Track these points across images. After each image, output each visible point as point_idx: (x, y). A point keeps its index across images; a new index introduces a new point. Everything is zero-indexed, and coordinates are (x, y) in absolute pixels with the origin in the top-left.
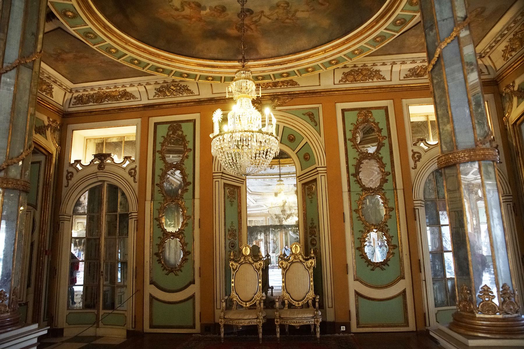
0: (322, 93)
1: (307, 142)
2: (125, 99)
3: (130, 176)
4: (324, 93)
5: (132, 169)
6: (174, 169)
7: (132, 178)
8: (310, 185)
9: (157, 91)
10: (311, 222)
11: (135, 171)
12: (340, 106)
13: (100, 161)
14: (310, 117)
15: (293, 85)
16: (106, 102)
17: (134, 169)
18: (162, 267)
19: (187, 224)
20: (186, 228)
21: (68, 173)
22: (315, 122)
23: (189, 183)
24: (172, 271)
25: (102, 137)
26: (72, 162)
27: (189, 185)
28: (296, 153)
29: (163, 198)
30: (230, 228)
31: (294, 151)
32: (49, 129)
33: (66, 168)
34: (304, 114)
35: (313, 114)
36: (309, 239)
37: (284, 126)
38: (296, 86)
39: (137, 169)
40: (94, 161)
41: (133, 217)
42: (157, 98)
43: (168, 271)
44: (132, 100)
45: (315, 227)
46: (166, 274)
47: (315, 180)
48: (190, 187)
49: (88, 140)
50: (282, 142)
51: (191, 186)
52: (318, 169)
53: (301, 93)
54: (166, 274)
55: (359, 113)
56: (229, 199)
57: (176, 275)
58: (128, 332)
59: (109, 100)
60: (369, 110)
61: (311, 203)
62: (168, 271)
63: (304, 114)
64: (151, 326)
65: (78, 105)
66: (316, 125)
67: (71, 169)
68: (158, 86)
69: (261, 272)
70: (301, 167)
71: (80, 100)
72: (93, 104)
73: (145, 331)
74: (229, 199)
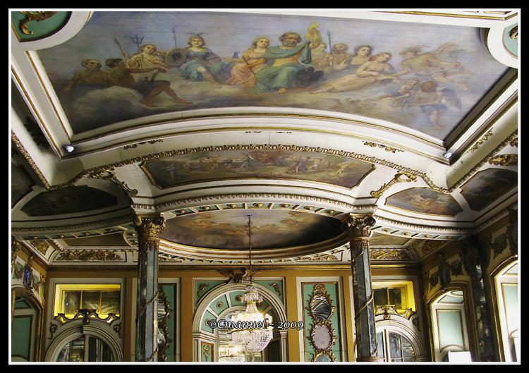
5: (117, 325)
11: (120, 328)
12: (300, 280)
21: (52, 325)
22: (279, 292)
26: (56, 315)
33: (49, 320)
39: (122, 326)
55: (314, 287)
60: (322, 284)
66: (280, 295)
67: (54, 322)
71: (66, 256)
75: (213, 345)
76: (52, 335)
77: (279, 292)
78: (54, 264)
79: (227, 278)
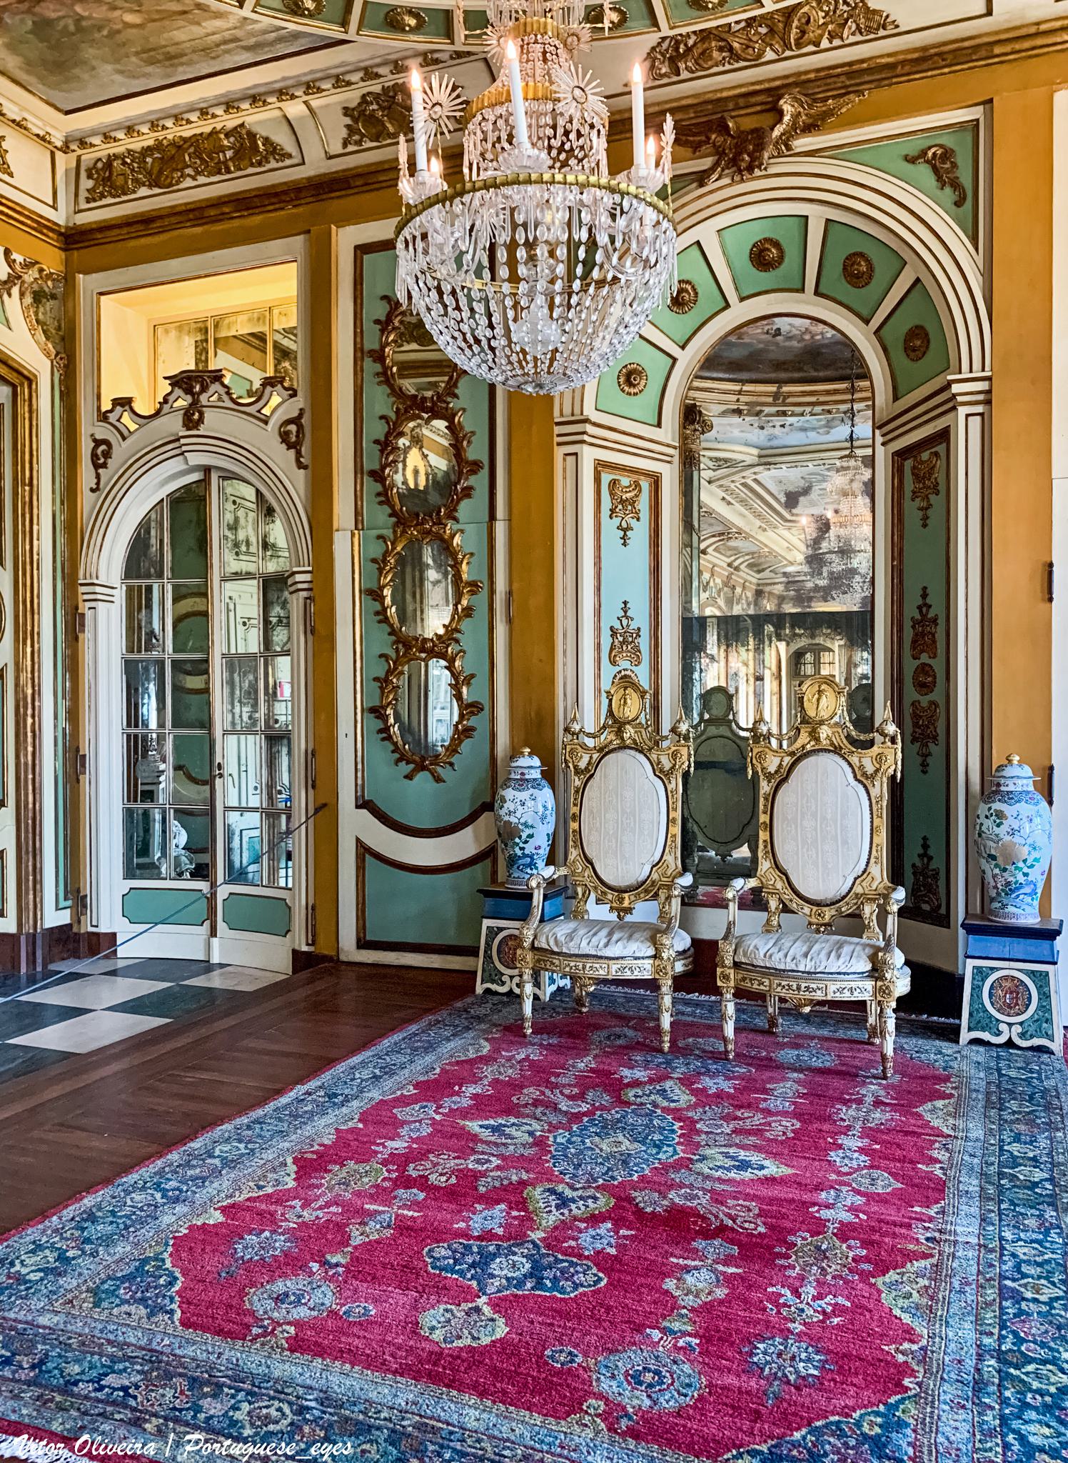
0: (997, 50)
1: (918, 280)
2: (252, 165)
3: (284, 446)
4: (1008, 48)
6: (426, 416)
7: (292, 453)
8: (925, 456)
9: (352, 117)
10: (920, 602)
11: (300, 428)
13: (189, 398)
14: (936, 170)
15: (870, 30)
16: (189, 182)
17: (296, 421)
18: (393, 752)
19: (468, 611)
20: (465, 625)
21: (98, 443)
22: (956, 185)
23: (475, 466)
24: (424, 768)
25: (202, 316)
27: (474, 472)
28: (876, 332)
29: (394, 519)
30: (617, 625)
31: (867, 322)
32: (15, 291)
33: (88, 428)
34: (911, 160)
35: (947, 154)
36: (910, 666)
37: (828, 220)
38: (882, 33)
40: (171, 398)
41: (300, 586)
42: (356, 148)
43: (412, 766)
44: (273, 164)
45: (935, 621)
46: (406, 777)
47: (944, 436)
48: (479, 482)
49: (160, 330)
50: (822, 289)
51: (485, 473)
52: (956, 388)
53: (903, 62)
54: (406, 777)
56: (616, 521)
57: (438, 779)
58: (296, 954)
59: (198, 173)
61: (925, 526)
62: (412, 766)
63: (911, 160)
64: (363, 944)
65: (104, 202)
66: (959, 204)
67: (102, 432)
68: (351, 97)
69: (677, 784)
70: (895, 388)
72: (150, 192)
73: (343, 958)
74: (616, 521)
75: (656, 481)
76: (98, 476)
77: (956, 185)
78: (83, 219)
79: (707, 163)
